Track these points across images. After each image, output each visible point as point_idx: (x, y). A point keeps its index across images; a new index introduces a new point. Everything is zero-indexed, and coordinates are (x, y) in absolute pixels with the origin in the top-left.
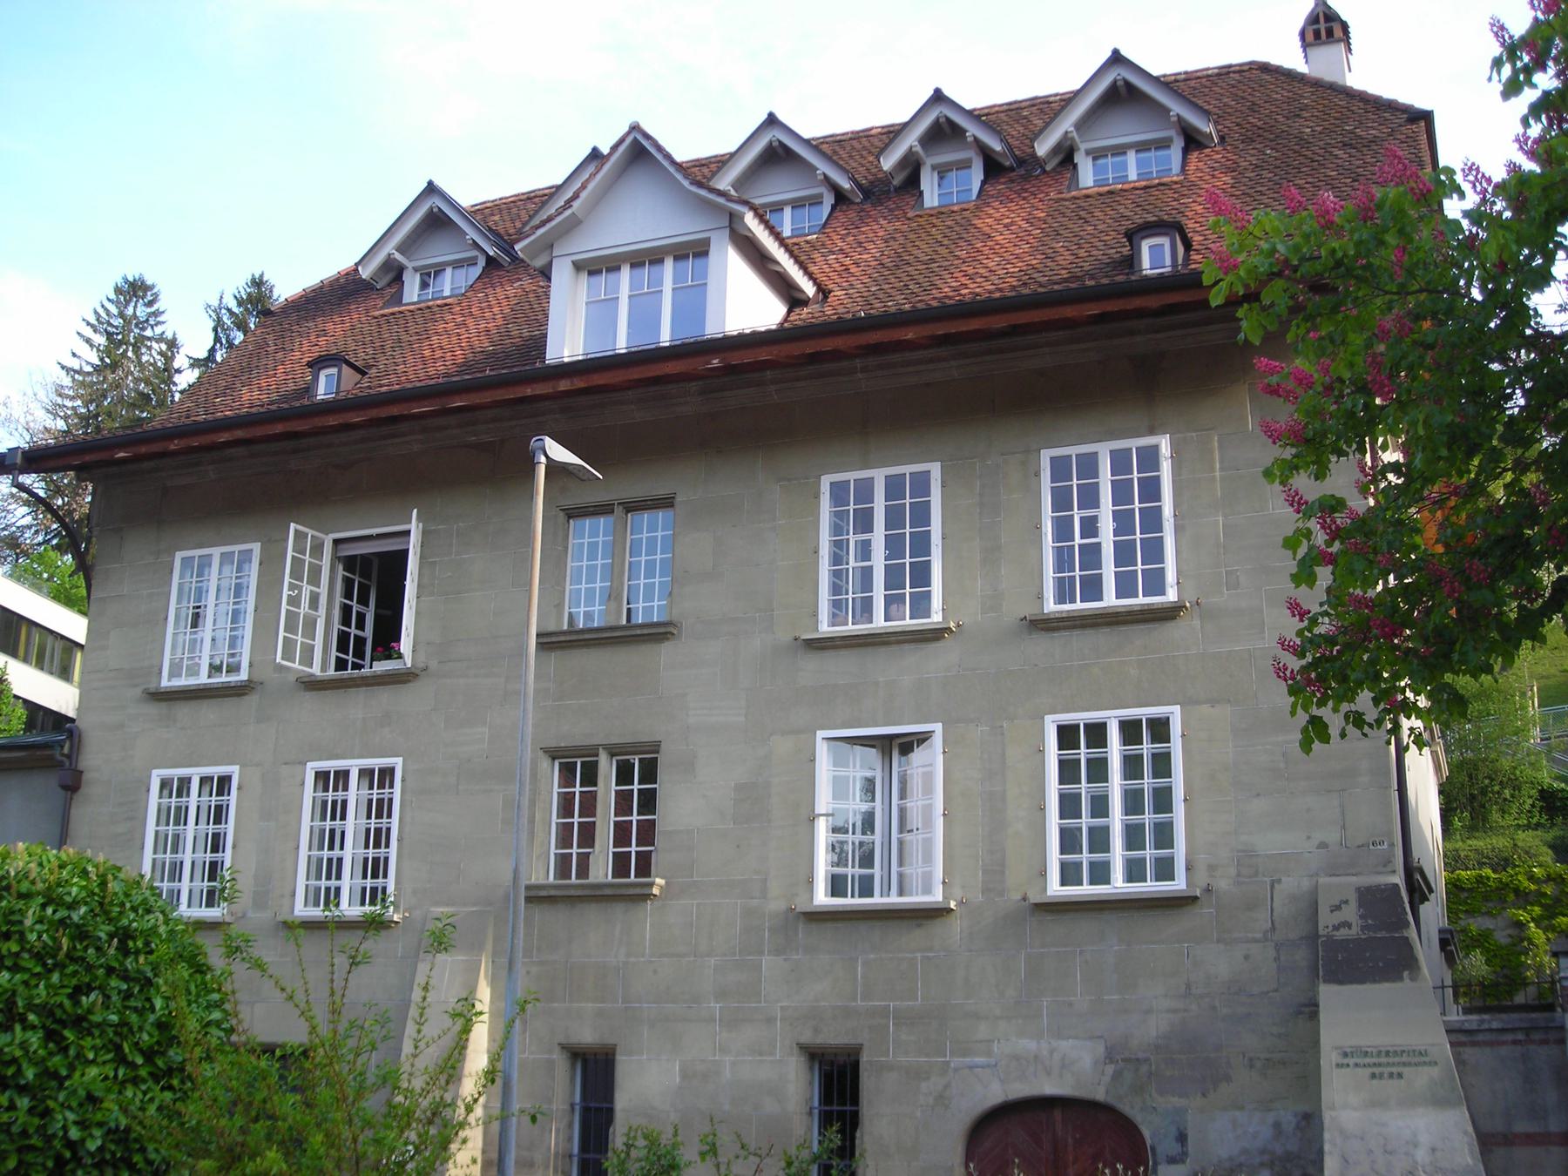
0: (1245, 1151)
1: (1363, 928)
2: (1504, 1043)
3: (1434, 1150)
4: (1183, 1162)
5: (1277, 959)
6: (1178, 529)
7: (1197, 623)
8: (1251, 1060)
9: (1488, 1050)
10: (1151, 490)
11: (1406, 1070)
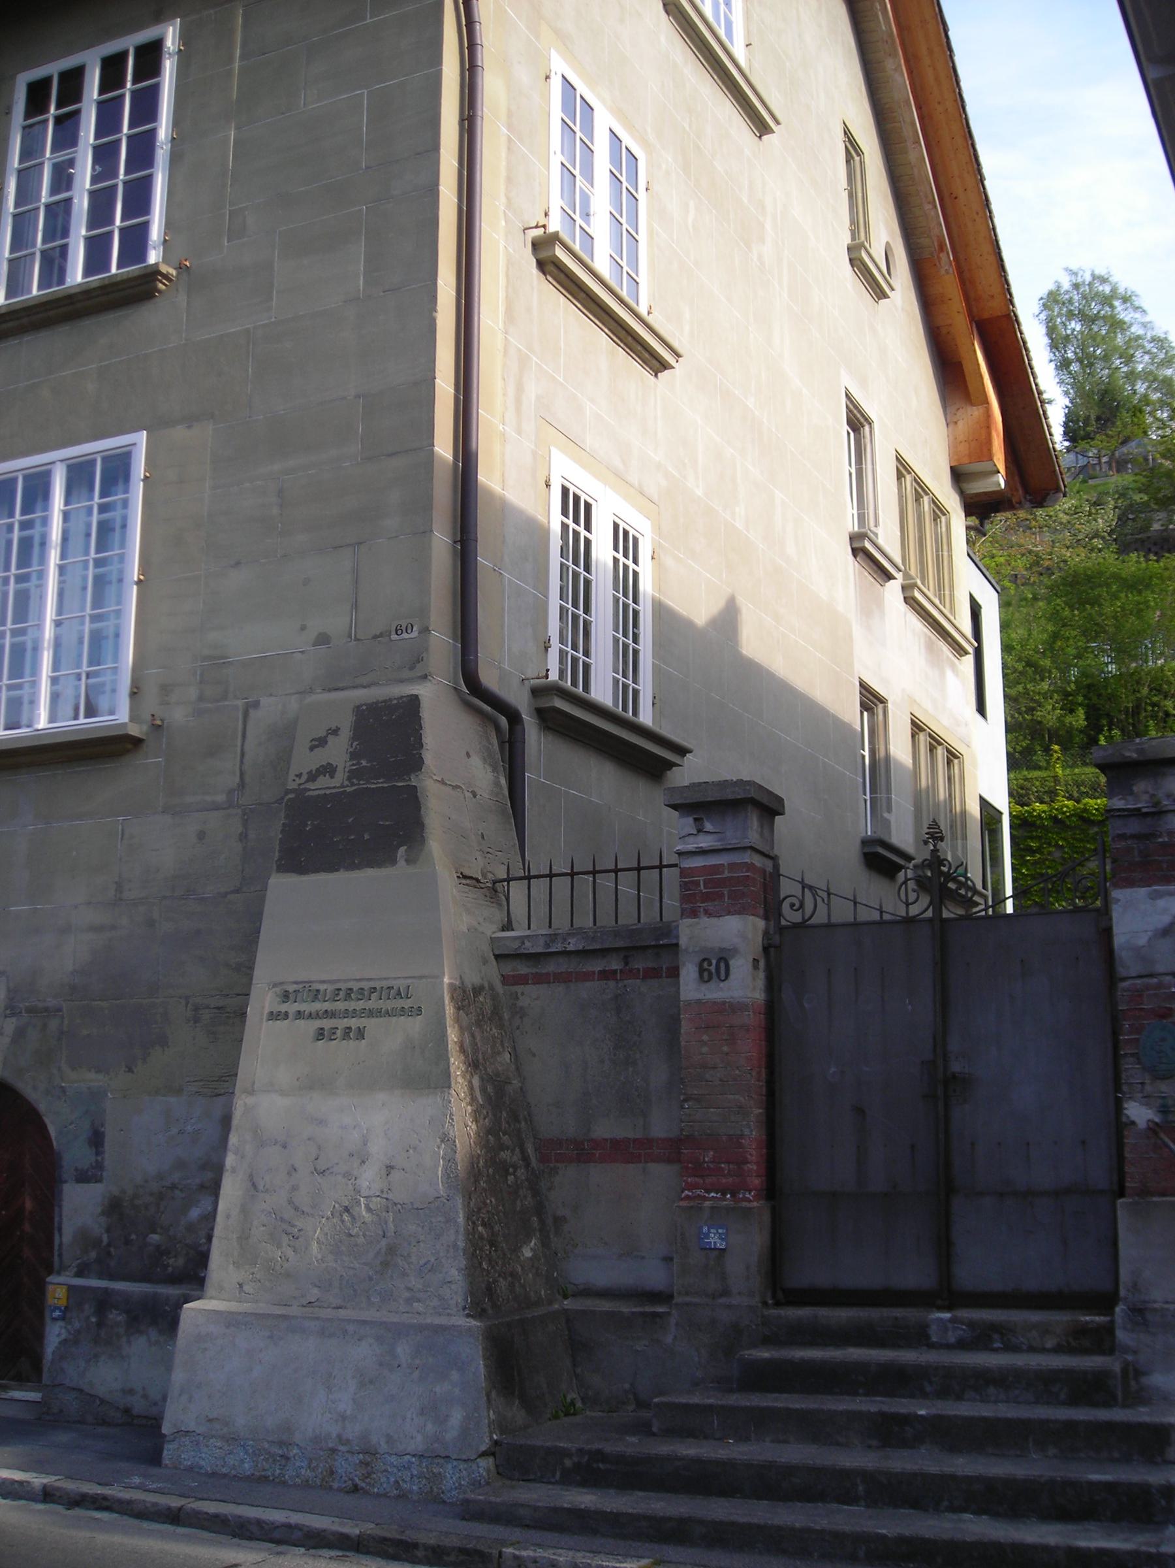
0: (181, 1165)
1: (353, 775)
2: (587, 977)
3: (390, 1168)
4: (99, 1180)
5: (243, 837)
6: (175, 158)
7: (182, 299)
8: (196, 1009)
9: (560, 989)
10: (146, 107)
11: (370, 1024)
